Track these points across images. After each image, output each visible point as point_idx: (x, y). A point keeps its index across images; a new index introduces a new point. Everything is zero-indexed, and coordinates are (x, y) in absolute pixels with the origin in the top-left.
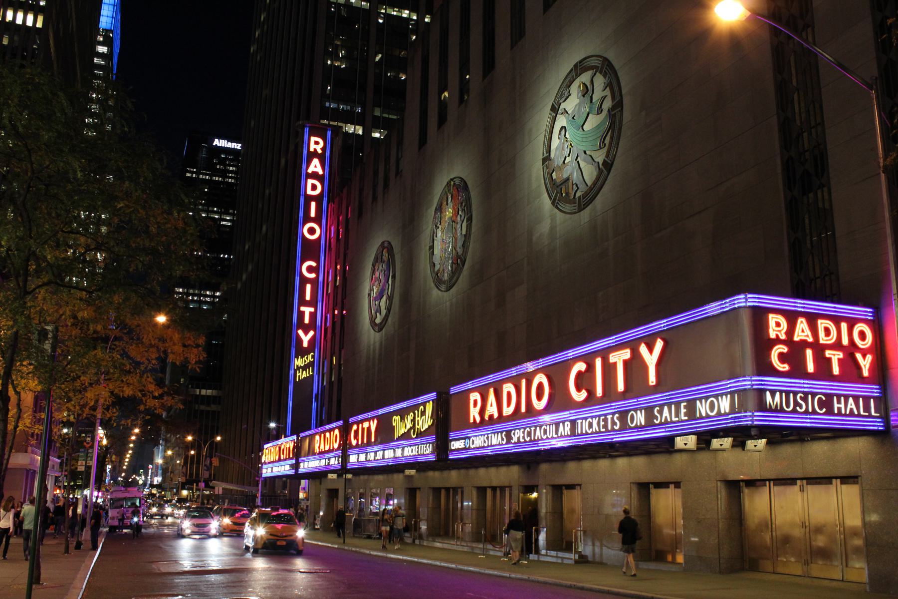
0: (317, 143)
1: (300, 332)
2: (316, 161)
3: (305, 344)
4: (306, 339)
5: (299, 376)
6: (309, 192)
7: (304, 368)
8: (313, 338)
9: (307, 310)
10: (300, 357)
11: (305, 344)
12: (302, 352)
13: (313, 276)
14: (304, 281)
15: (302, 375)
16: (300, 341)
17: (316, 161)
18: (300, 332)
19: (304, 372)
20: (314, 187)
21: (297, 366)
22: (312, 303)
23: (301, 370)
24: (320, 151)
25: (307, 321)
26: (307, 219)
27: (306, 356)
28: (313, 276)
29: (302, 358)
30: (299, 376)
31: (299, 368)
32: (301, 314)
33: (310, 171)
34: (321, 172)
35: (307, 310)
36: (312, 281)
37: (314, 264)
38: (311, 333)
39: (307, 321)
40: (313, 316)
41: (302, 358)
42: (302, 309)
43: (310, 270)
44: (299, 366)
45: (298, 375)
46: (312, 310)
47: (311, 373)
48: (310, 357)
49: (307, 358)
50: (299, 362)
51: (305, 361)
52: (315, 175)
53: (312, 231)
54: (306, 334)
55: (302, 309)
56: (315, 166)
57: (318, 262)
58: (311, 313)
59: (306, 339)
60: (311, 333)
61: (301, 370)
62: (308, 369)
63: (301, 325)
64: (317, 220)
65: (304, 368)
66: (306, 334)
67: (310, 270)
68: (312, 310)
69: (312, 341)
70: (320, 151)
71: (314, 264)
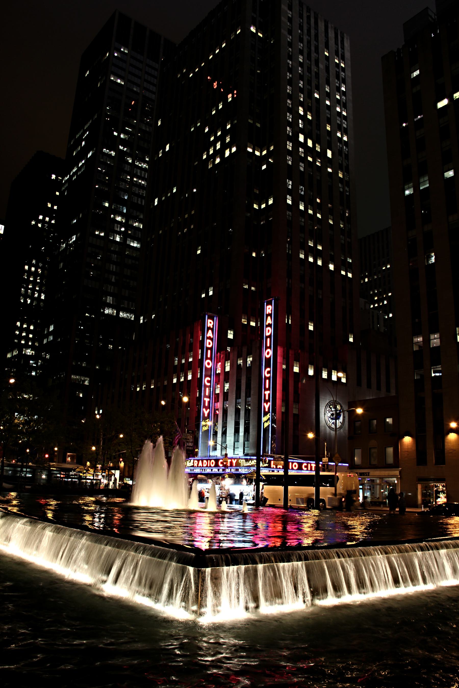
0: (210, 323)
1: (204, 409)
2: (210, 331)
3: (206, 415)
4: (206, 412)
6: (208, 346)
8: (209, 411)
9: (207, 400)
11: (206, 415)
13: (209, 384)
14: (206, 386)
16: (204, 414)
17: (210, 331)
20: (209, 344)
22: (209, 397)
24: (212, 327)
25: (207, 405)
26: (207, 358)
31: (203, 426)
32: (204, 402)
33: (208, 336)
34: (212, 337)
35: (207, 400)
37: (209, 379)
38: (208, 410)
39: (207, 405)
40: (209, 402)
42: (205, 399)
43: (208, 381)
46: (208, 400)
52: (209, 338)
53: (209, 364)
54: (206, 410)
55: (205, 399)
56: (210, 334)
57: (211, 378)
59: (206, 412)
60: (208, 410)
63: (204, 407)
64: (211, 359)
66: (206, 410)
67: (208, 381)
68: (208, 400)
69: (209, 414)
70: (212, 327)
71: (209, 379)
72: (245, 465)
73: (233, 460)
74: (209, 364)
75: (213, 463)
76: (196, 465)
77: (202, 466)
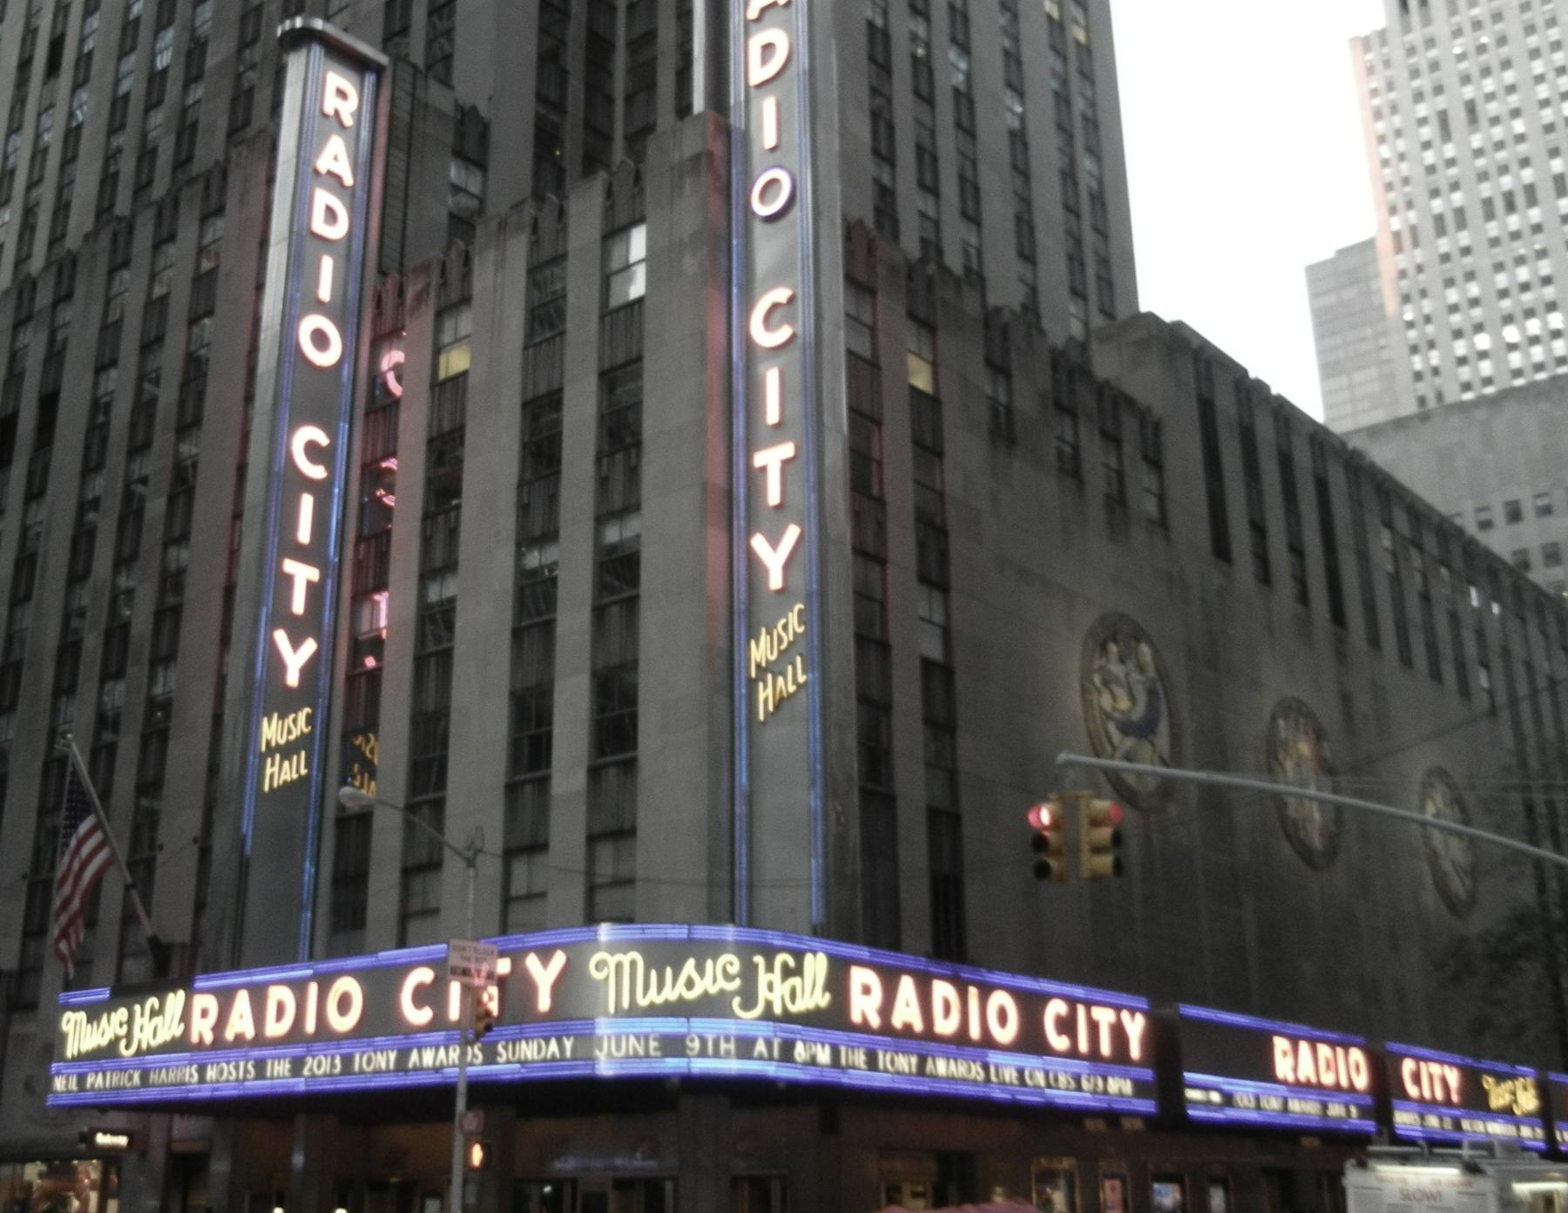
1: (281, 637)
3: (293, 679)
4: (295, 658)
5: (272, 776)
7: (287, 751)
9: (302, 574)
10: (276, 715)
11: (293, 679)
12: (286, 703)
13: (317, 472)
15: (281, 773)
18: (281, 637)
19: (286, 764)
20: (331, 215)
21: (268, 743)
23: (278, 757)
25: (298, 605)
27: (292, 716)
28: (317, 472)
29: (282, 717)
30: (272, 776)
31: (271, 750)
36: (320, 490)
37: (323, 439)
38: (310, 647)
39: (298, 605)
41: (282, 717)
42: (290, 566)
43: (312, 450)
44: (273, 744)
45: (268, 771)
46: (313, 574)
47: (303, 771)
48: (302, 716)
49: (295, 721)
50: (272, 731)
51: (289, 732)
54: (296, 643)
55: (290, 566)
58: (310, 584)
61: (278, 757)
62: (295, 758)
65: (287, 751)
66: (296, 643)
67: (312, 450)
68: (313, 574)
71: (323, 439)
72: (643, 1002)
73: (532, 962)
74: (320, 339)
75: (344, 1004)
76: (202, 1029)
77: (250, 1033)
